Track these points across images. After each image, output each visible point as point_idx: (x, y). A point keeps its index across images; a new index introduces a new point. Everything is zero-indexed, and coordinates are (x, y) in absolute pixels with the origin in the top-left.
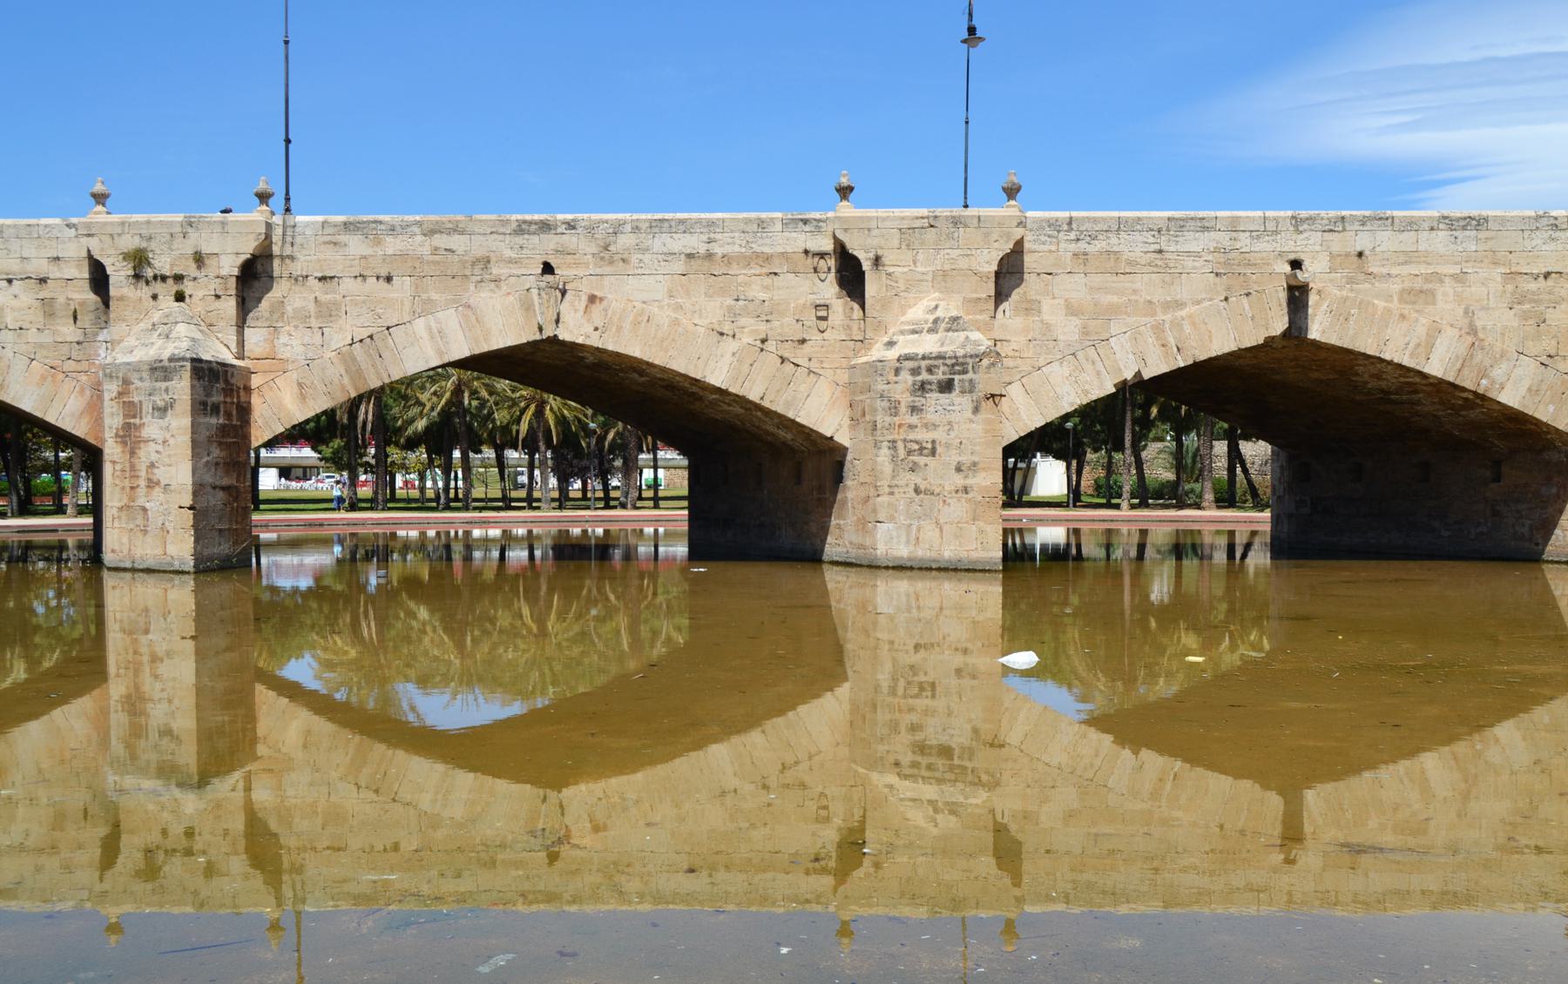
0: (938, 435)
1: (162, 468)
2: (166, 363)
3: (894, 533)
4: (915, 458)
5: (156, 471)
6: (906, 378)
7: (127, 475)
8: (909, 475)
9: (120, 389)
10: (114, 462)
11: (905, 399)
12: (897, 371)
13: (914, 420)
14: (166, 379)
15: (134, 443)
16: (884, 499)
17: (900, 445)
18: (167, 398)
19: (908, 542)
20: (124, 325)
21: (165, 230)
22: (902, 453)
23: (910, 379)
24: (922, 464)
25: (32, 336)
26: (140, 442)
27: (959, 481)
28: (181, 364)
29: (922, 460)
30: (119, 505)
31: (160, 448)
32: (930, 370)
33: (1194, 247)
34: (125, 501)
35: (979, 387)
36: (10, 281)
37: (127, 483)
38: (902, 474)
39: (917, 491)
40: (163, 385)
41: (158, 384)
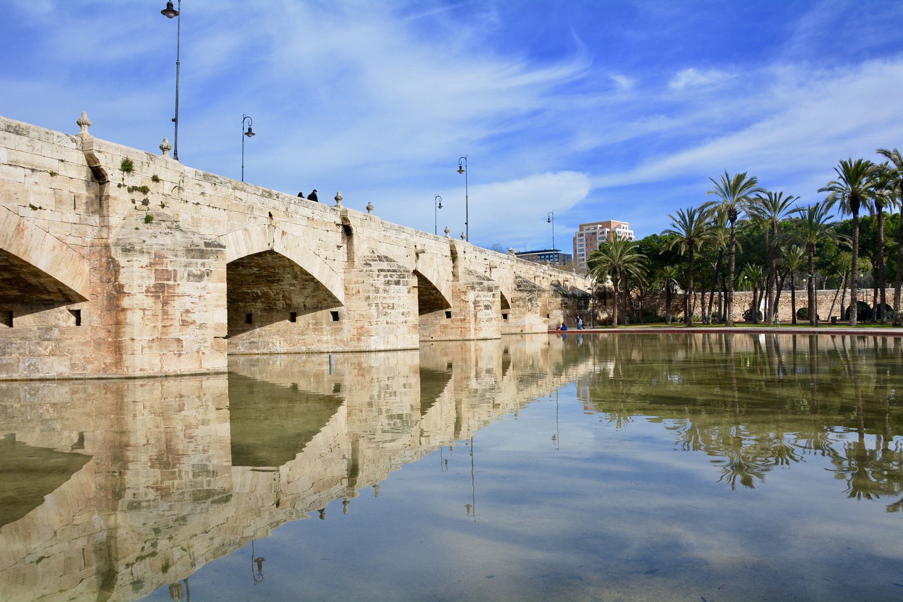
0: (395, 301)
1: (197, 313)
2: (204, 248)
3: (378, 340)
4: (387, 310)
5: (190, 315)
6: (382, 279)
7: (160, 317)
8: (384, 317)
9: (152, 261)
10: (144, 310)
11: (382, 287)
12: (378, 276)
13: (385, 295)
14: (202, 257)
15: (167, 296)
16: (374, 326)
17: (380, 305)
18: (203, 269)
19: (384, 343)
20: (117, 216)
21: (139, 159)
22: (381, 308)
23: (384, 279)
24: (389, 312)
25: (46, 214)
26: (174, 296)
27: (403, 319)
28: (218, 249)
29: (389, 311)
30: (148, 338)
31: (197, 300)
32: (391, 276)
33: (402, 237)
34: (156, 335)
35: (410, 284)
36: (33, 170)
37: (159, 325)
38: (381, 317)
39: (387, 323)
40: (200, 261)
41: (194, 260)
